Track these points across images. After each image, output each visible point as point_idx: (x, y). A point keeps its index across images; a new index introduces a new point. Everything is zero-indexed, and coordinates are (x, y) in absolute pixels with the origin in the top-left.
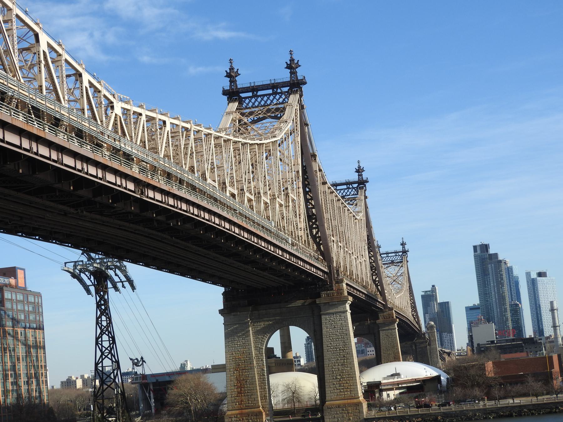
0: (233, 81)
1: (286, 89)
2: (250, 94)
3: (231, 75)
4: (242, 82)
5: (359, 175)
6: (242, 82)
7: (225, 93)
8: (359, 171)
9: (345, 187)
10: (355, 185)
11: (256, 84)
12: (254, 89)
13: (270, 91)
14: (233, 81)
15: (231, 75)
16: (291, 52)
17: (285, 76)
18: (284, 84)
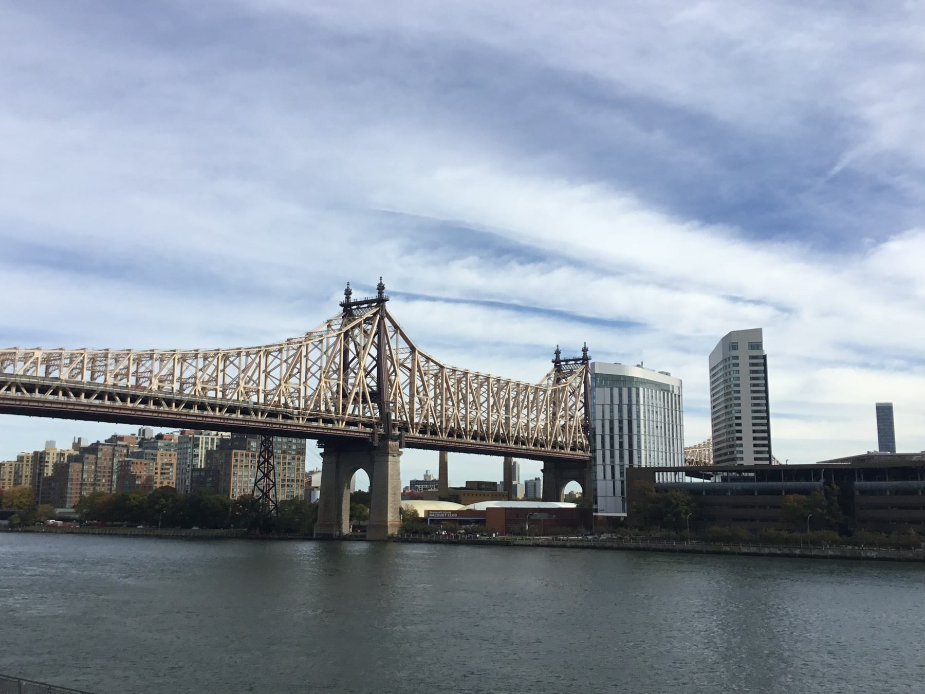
0: (348, 298)
1: (375, 304)
2: (355, 307)
3: (348, 293)
4: (353, 298)
5: (584, 353)
6: (353, 298)
7: (341, 305)
8: (585, 350)
9: (573, 362)
10: (581, 361)
11: (358, 300)
12: (358, 303)
13: (366, 305)
14: (348, 298)
15: (348, 293)
16: (381, 278)
17: (374, 295)
18: (372, 301)
